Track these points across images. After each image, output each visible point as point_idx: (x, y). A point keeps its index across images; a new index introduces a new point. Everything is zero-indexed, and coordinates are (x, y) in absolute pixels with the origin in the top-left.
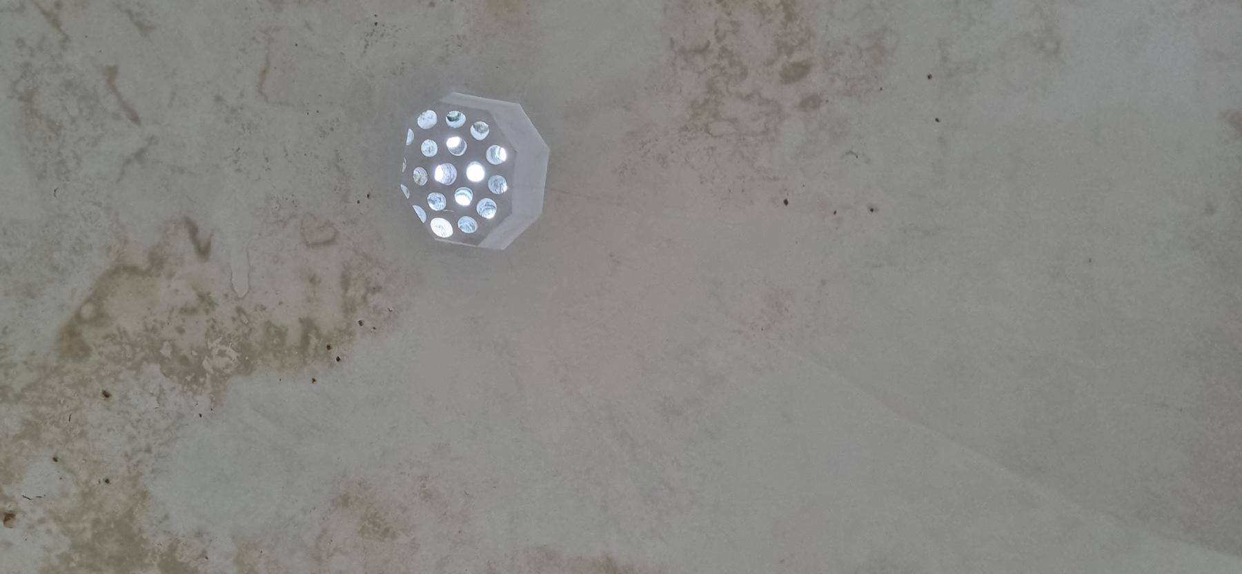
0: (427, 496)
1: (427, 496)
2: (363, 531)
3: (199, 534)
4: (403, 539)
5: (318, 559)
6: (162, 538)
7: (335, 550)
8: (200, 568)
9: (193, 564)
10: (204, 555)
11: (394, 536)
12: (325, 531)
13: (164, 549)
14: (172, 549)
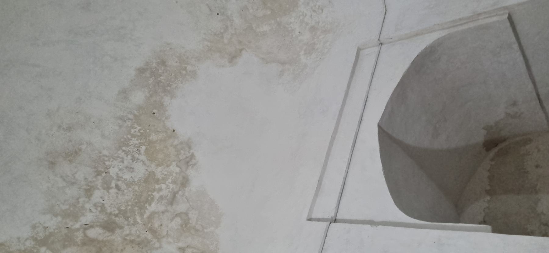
0: (70, 129)
1: (70, 129)
2: (71, 161)
3: (34, 227)
4: (84, 147)
5: (73, 184)
6: (28, 243)
7: (73, 175)
8: (50, 231)
9: (47, 233)
10: (45, 228)
11: (80, 150)
12: (61, 177)
13: (33, 243)
14: (35, 240)
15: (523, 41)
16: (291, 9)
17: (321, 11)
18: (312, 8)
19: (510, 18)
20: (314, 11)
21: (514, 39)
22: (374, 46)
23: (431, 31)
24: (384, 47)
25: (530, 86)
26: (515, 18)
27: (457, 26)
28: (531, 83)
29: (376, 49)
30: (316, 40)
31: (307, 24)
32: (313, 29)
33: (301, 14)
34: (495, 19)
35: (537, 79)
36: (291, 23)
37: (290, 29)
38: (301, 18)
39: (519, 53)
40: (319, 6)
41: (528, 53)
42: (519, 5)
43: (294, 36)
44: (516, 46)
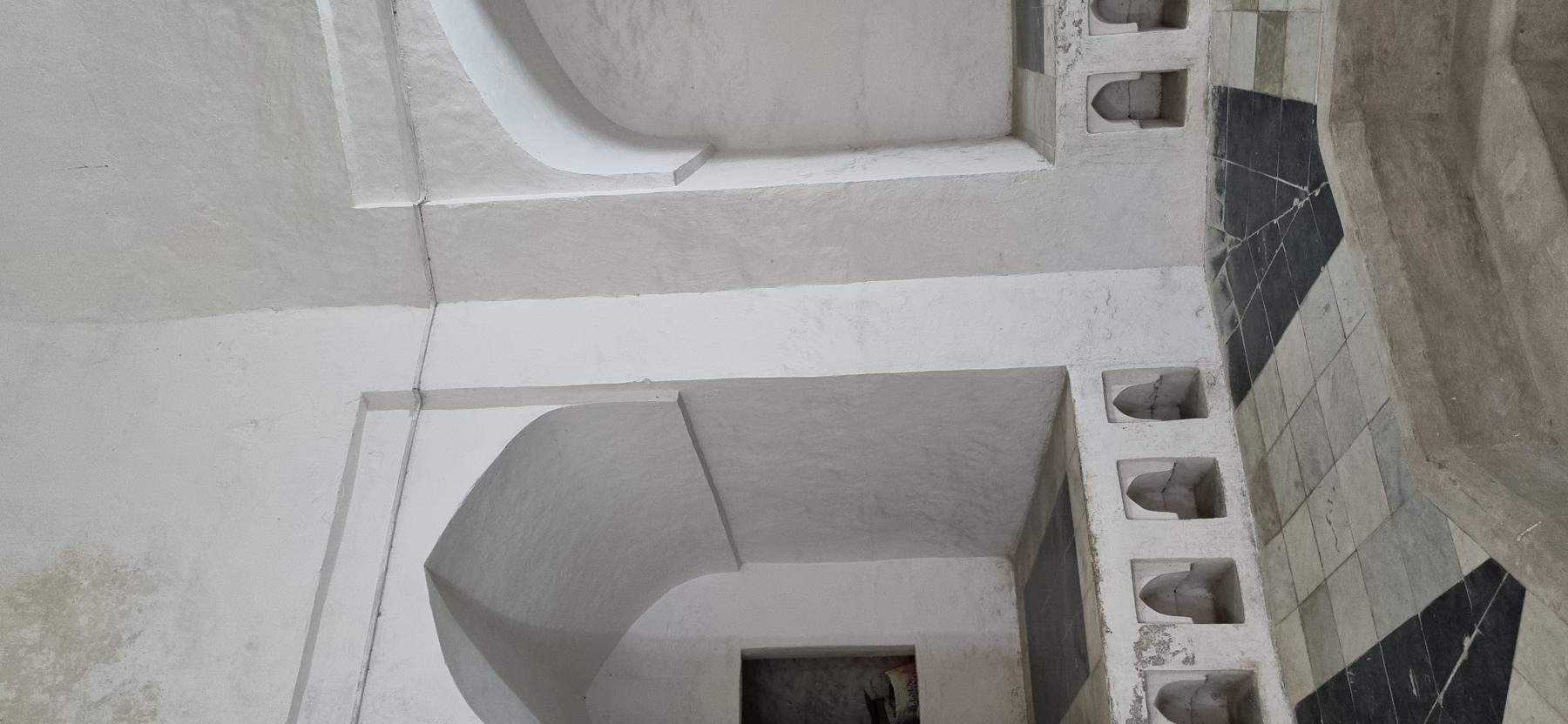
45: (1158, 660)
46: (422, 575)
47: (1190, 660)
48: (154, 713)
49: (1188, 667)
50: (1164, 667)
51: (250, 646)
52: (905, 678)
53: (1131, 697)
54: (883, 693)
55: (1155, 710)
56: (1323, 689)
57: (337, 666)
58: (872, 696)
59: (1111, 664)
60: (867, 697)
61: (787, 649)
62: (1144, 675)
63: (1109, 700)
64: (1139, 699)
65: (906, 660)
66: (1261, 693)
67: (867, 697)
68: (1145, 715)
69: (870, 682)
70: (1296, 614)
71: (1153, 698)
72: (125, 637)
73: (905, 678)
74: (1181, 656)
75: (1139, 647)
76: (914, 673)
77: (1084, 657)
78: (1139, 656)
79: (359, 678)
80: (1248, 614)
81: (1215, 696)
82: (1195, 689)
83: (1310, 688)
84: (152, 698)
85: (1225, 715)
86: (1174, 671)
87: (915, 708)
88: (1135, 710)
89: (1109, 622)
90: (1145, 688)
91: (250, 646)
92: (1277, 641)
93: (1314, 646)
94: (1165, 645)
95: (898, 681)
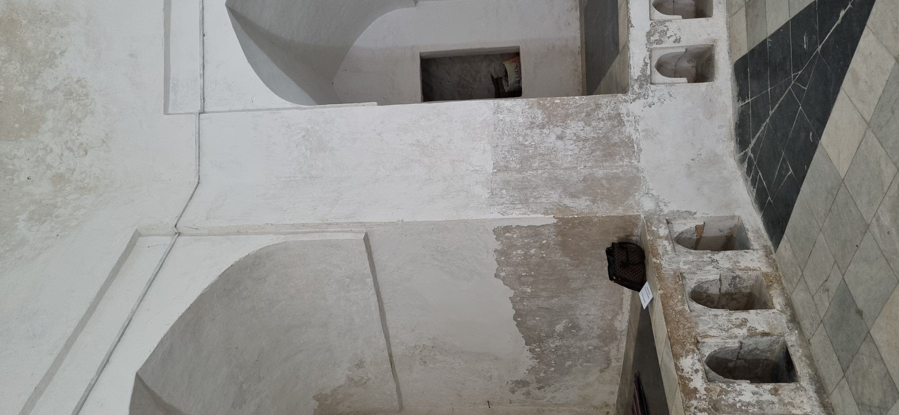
15: (381, 277)
16: (24, 134)
17: (82, 152)
18: (67, 142)
19: (366, 239)
20: (71, 150)
21: (368, 271)
22: (165, 235)
23: (260, 231)
24: (181, 238)
25: (383, 341)
26: (373, 241)
27: (298, 233)
28: (383, 337)
29: (168, 240)
30: (59, 199)
31: (49, 167)
32: (59, 179)
33: (41, 146)
34: (348, 236)
35: (392, 332)
36: (15, 156)
37: (10, 167)
38: (40, 153)
39: (373, 291)
40: (81, 144)
41: (384, 296)
42: (380, 224)
43: (16, 182)
44: (370, 280)
45: (659, 42)
46: (225, 9)
47: (678, 41)
48: (87, 95)
49: (676, 45)
50: (663, 45)
51: (131, 55)
52: (514, 65)
53: (642, 63)
54: (501, 75)
55: (655, 70)
56: (752, 52)
57: (185, 66)
58: (495, 77)
59: (632, 45)
60: (492, 77)
61: (447, 52)
62: (650, 51)
63: (629, 66)
64: (646, 64)
65: (514, 55)
66: (716, 57)
67: (492, 77)
68: (649, 73)
69: (495, 69)
70: (743, 12)
71: (654, 63)
72: (57, 52)
73: (514, 65)
74: (673, 38)
75: (649, 35)
76: (519, 62)
77: (617, 44)
78: (648, 39)
79: (199, 71)
80: (715, 11)
81: (689, 61)
82: (679, 57)
83: (745, 51)
84: (83, 87)
85: (694, 71)
86: (669, 47)
87: (519, 82)
88: (643, 71)
89: (633, 21)
90: (650, 58)
91: (131, 55)
92: (730, 27)
93: (750, 27)
94: (664, 33)
95: (510, 67)
